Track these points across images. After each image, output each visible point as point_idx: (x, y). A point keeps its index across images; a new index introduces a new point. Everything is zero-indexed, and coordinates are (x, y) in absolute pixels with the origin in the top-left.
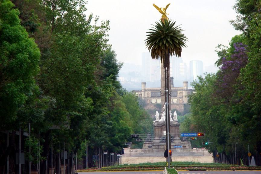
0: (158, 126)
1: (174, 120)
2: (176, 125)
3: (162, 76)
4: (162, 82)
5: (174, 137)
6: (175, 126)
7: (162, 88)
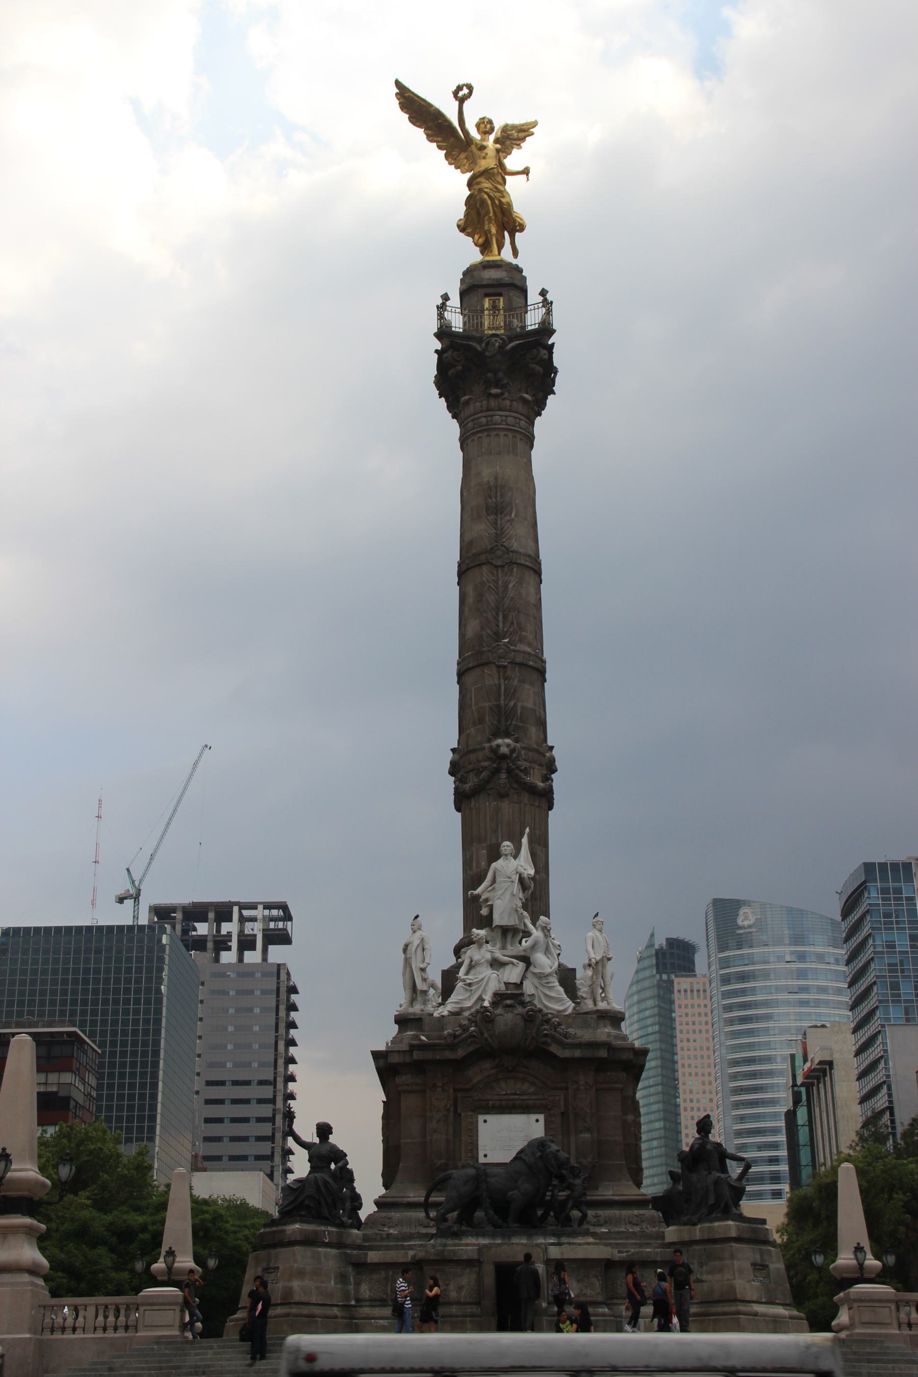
0: (418, 1067)
1: (589, 1005)
2: (603, 1053)
3: (473, 626)
4: (469, 679)
5: (592, 1181)
6: (600, 1065)
7: (472, 731)
